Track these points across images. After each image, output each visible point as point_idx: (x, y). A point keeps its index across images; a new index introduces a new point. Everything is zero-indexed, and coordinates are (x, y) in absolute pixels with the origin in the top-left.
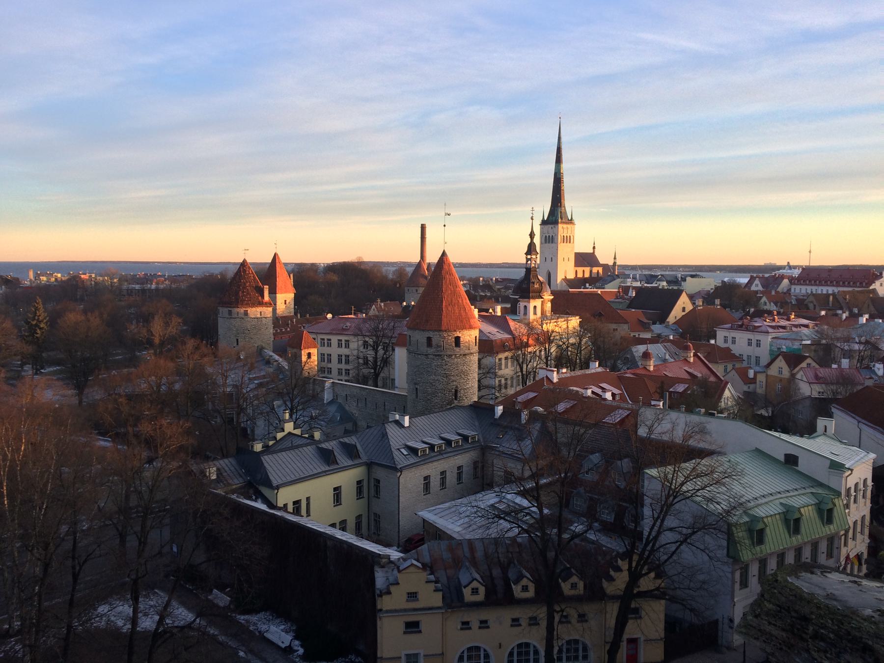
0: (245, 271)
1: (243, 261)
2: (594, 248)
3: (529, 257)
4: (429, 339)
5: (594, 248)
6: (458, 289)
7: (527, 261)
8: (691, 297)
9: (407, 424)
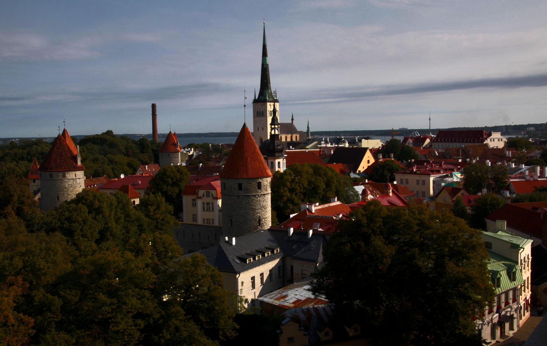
1: (59, 136)
2: (292, 120)
3: (273, 127)
4: (240, 186)
5: (292, 120)
6: (257, 149)
7: (271, 130)
8: (375, 153)
9: (234, 243)
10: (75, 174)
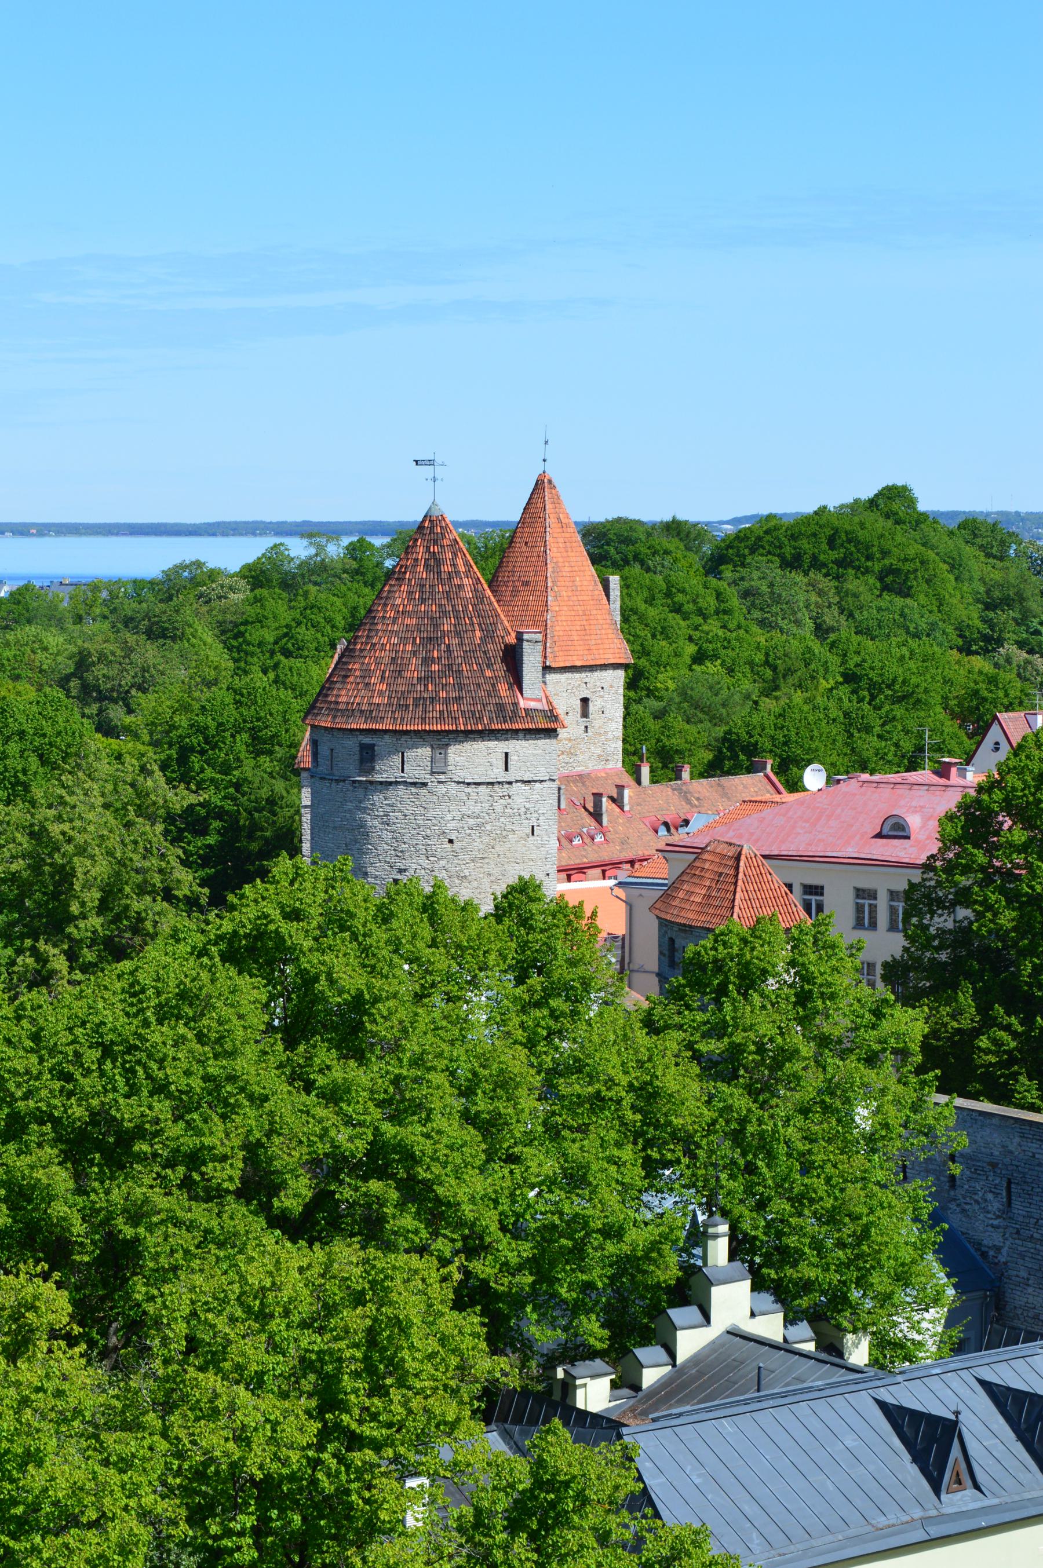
0: (434, 563)
10: (507, 754)
